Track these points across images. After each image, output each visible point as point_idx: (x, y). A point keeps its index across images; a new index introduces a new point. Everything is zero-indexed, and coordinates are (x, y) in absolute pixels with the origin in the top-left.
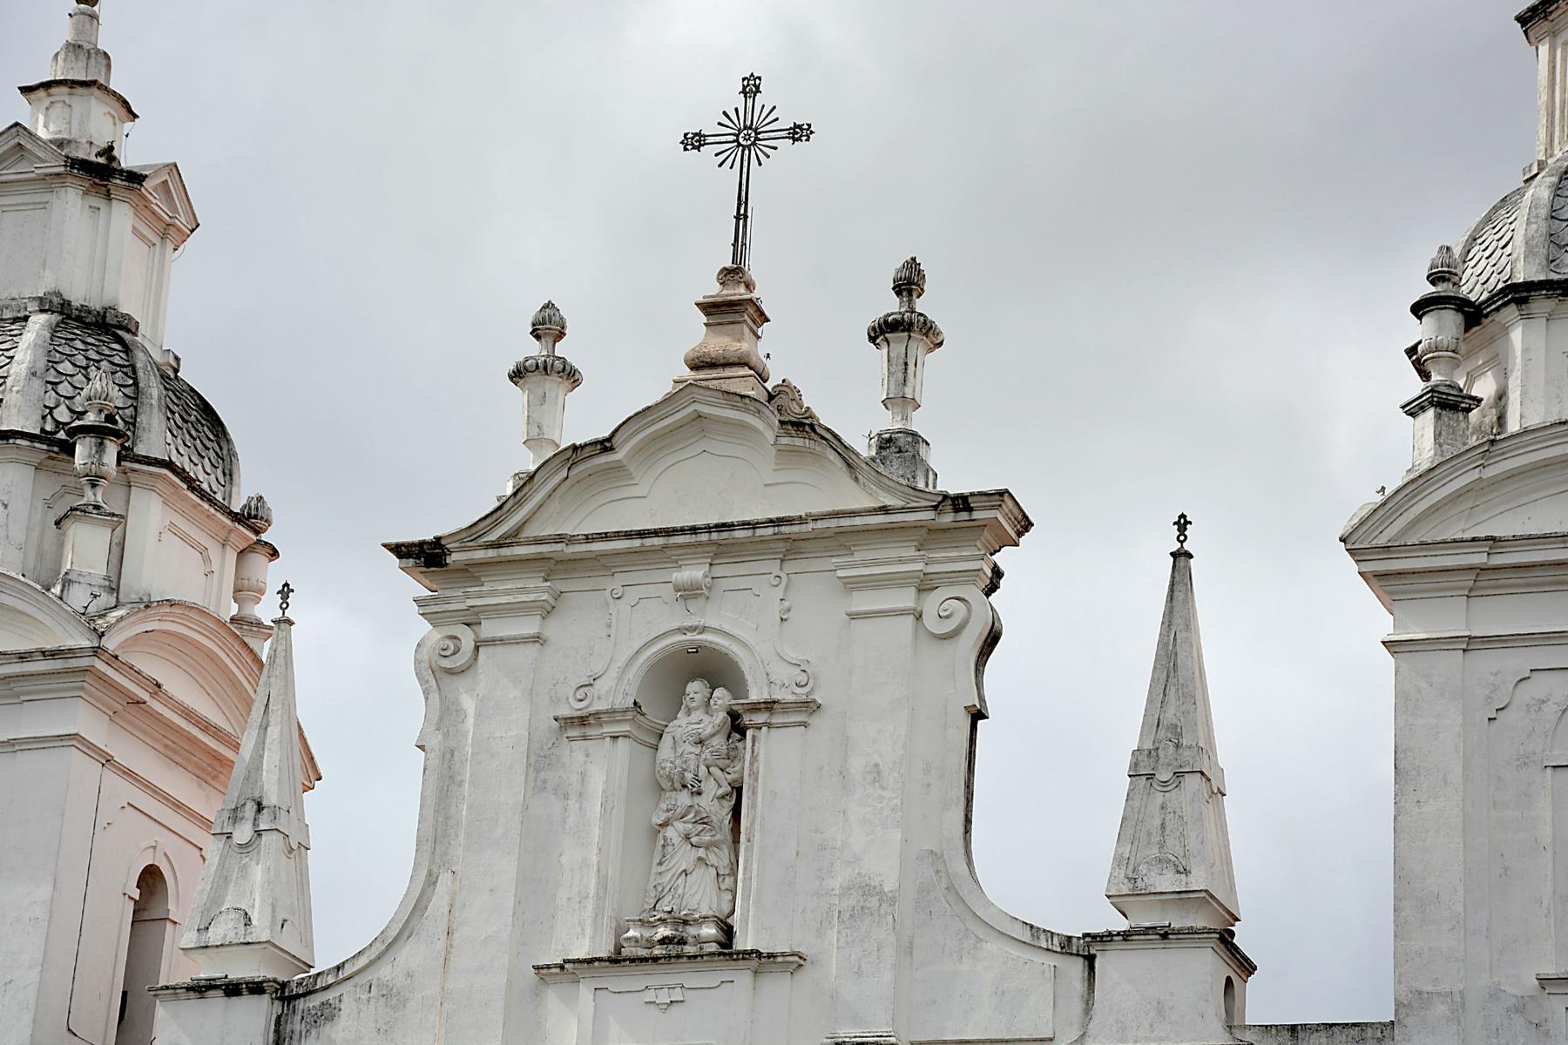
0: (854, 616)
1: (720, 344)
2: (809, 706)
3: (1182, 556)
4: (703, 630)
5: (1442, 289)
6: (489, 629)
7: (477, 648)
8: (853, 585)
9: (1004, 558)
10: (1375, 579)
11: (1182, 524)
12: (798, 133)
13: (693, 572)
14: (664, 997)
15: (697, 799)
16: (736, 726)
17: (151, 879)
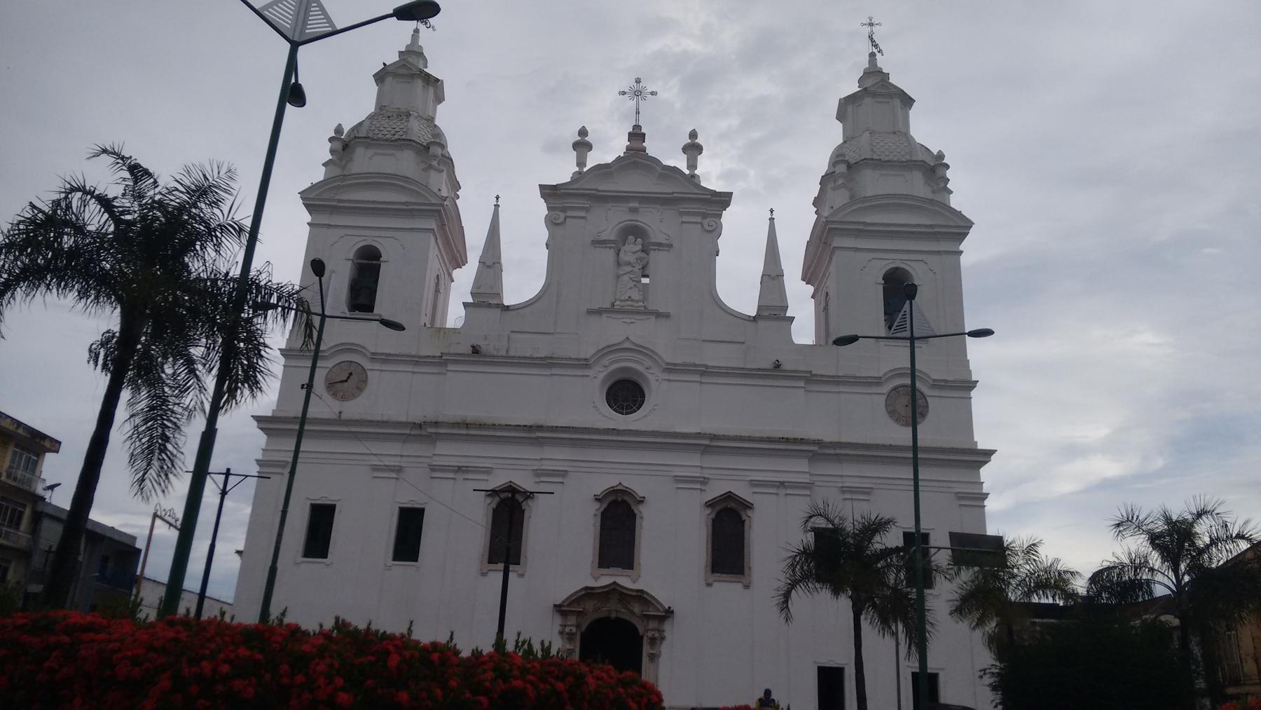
0: (682, 222)
2: (671, 246)
3: (772, 219)
4: (637, 221)
6: (569, 213)
7: (565, 219)
8: (682, 214)
15: (634, 269)
16: (645, 250)
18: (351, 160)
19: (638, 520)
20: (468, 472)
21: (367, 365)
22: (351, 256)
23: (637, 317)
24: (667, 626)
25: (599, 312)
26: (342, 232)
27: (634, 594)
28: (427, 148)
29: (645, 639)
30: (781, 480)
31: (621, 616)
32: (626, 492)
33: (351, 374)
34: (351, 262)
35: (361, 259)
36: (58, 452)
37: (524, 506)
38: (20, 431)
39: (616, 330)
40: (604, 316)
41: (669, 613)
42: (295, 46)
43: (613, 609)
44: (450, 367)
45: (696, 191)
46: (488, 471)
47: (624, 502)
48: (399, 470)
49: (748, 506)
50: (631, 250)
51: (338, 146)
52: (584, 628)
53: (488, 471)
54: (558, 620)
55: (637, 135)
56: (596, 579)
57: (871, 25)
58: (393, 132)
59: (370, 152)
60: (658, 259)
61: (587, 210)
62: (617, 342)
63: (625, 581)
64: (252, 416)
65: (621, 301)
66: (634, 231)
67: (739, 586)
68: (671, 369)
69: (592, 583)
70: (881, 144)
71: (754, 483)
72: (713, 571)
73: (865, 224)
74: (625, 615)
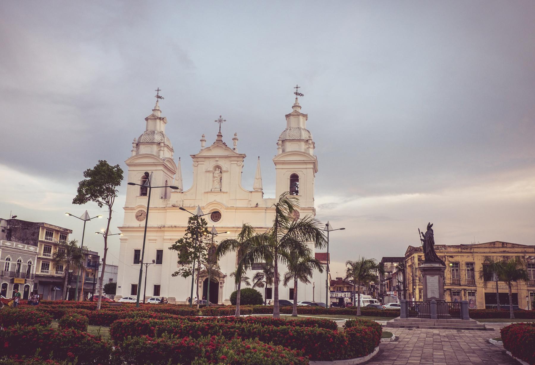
1: (219, 139)
5: (281, 139)
8: (231, 161)
9: (244, 159)
10: (275, 163)
12: (225, 121)
13: (217, 159)
14: (216, 195)
16: (221, 172)
17: (166, 181)
18: (139, 148)
20: (173, 240)
22: (140, 179)
23: (218, 193)
24: (225, 279)
25: (207, 193)
26: (138, 172)
28: (159, 144)
33: (142, 214)
34: (140, 181)
35: (144, 179)
36: (72, 233)
38: (61, 230)
39: (212, 198)
40: (209, 194)
42: (85, 221)
44: (168, 211)
45: (235, 154)
48: (156, 240)
50: (218, 172)
51: (135, 145)
55: (220, 136)
57: (297, 88)
58: (150, 139)
59: (144, 146)
60: (224, 175)
61: (204, 161)
62: (212, 201)
64: (118, 227)
65: (214, 189)
66: (218, 167)
68: (227, 208)
70: (293, 133)
73: (284, 161)
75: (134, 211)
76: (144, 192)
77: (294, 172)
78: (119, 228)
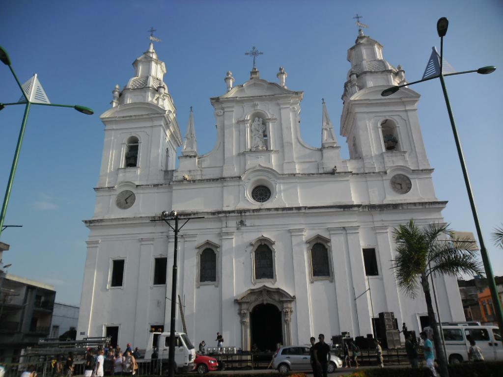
11: (323, 99)
19: (273, 254)
21: (134, 191)
27: (275, 290)
29: (282, 312)
30: (344, 226)
31: (269, 302)
32: (266, 240)
37: (216, 252)
39: (252, 162)
41: (294, 297)
43: (266, 300)
46: (195, 236)
47: (265, 245)
49: (328, 241)
52: (251, 310)
53: (195, 236)
54: (237, 307)
56: (254, 284)
60: (271, 126)
63: (269, 284)
66: (258, 115)
67: (327, 282)
69: (253, 288)
71: (328, 230)
72: (314, 276)
74: (271, 301)
75: (113, 193)
76: (132, 161)
77: (388, 118)
78: (86, 222)
